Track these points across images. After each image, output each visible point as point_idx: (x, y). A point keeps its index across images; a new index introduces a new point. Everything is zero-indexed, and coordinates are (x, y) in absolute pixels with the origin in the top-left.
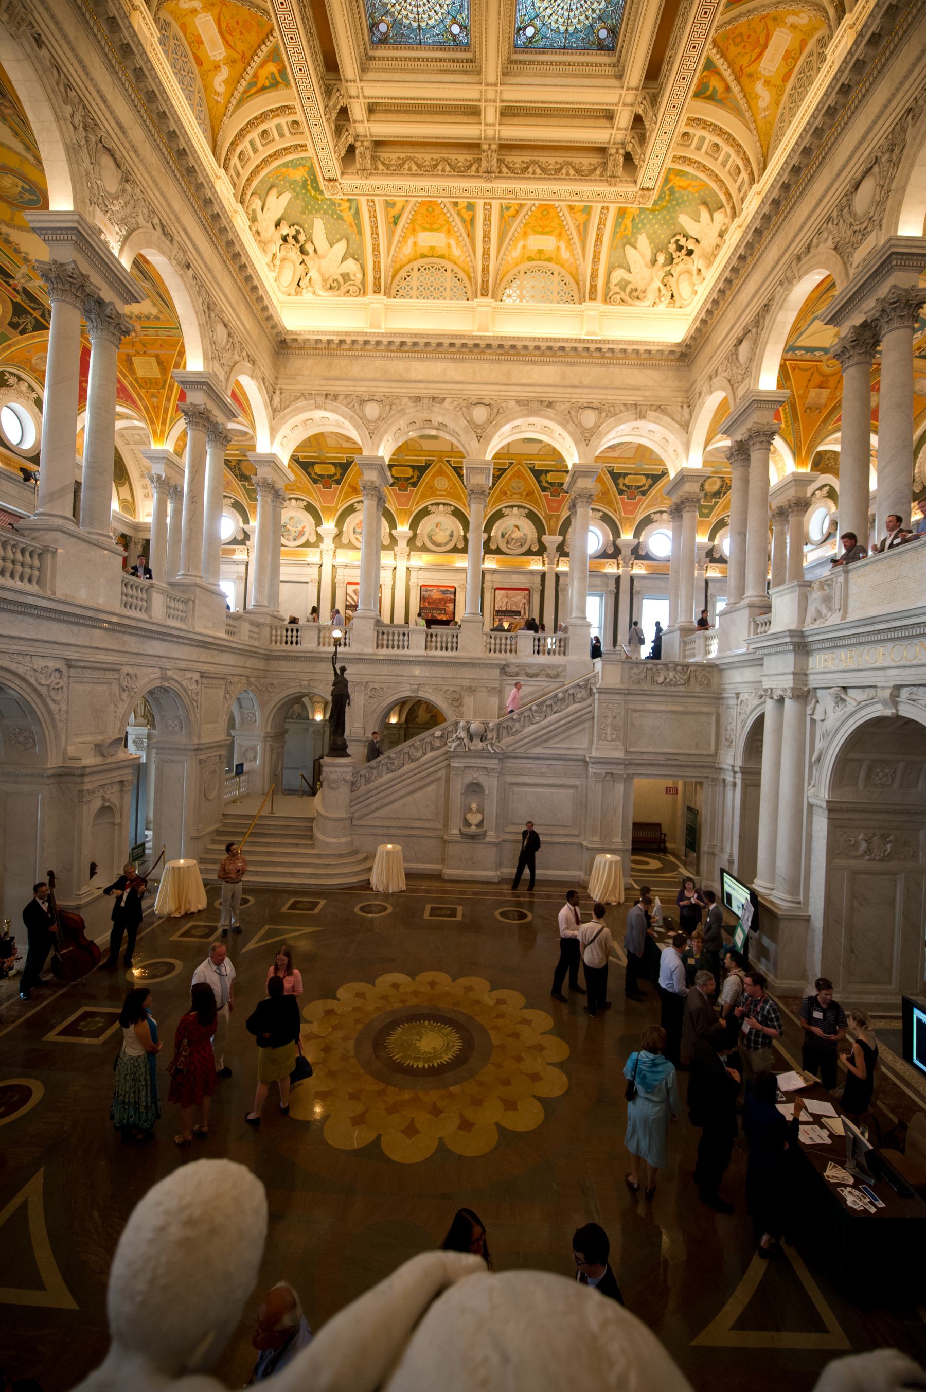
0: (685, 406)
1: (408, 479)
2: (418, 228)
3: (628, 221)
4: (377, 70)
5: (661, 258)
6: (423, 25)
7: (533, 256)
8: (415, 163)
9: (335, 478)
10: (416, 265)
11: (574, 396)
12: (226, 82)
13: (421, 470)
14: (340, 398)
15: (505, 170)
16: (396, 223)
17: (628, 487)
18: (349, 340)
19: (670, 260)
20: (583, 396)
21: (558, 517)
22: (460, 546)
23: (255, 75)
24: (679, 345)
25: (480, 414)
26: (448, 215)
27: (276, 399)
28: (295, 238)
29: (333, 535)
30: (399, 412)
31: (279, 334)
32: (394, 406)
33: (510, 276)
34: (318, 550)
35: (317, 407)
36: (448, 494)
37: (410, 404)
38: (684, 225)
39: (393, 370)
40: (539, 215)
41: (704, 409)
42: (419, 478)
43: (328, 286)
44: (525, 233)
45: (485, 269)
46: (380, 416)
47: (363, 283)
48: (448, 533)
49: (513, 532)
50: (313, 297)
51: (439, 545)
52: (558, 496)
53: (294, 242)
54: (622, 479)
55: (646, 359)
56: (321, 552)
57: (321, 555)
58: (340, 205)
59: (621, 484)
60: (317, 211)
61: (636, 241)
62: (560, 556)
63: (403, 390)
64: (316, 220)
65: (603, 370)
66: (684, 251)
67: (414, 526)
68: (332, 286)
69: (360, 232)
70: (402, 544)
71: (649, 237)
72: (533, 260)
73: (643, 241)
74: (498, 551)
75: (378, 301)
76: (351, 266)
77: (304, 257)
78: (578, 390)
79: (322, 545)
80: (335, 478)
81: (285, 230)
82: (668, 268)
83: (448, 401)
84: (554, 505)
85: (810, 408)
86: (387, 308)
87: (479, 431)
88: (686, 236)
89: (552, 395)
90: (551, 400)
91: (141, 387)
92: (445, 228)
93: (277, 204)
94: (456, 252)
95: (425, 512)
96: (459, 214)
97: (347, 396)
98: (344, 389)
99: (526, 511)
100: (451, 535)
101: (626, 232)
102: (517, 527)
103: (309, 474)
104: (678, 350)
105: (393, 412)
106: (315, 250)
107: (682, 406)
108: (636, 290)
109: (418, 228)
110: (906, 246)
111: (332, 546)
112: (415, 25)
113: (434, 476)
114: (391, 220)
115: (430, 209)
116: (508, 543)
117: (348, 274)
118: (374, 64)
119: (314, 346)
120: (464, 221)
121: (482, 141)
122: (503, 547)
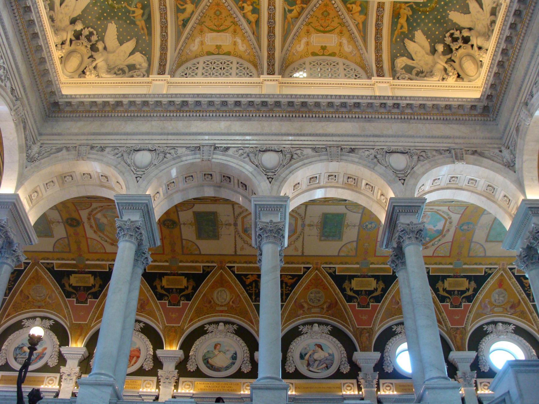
0: (503, 149)
1: (182, 290)
2: (206, 29)
3: (403, 21)
5: (440, 48)
7: (317, 51)
9: (93, 290)
11: (377, 144)
13: (197, 279)
14: (107, 150)
17: (449, 292)
18: (125, 101)
19: (448, 50)
21: (371, 332)
22: (247, 369)
24: (479, 100)
25: (270, 159)
26: (234, 16)
27: (35, 149)
29: (80, 356)
30: (174, 159)
31: (53, 93)
32: (168, 155)
33: (295, 65)
34: (58, 375)
36: (231, 310)
38: (455, 21)
39: (170, 128)
40: (320, 16)
41: (528, 138)
42: (195, 289)
44: (308, 32)
45: (271, 57)
46: (151, 164)
48: (229, 355)
49: (314, 352)
50: (97, 78)
51: (218, 370)
52: (368, 306)
54: (440, 283)
55: (449, 114)
56: (61, 377)
57: (60, 381)
59: (441, 289)
60: (112, 18)
61: (413, 36)
62: (380, 378)
64: (110, 25)
65: (405, 125)
66: (460, 41)
67: (186, 346)
70: (169, 368)
71: (425, 33)
72: (317, 55)
73: (419, 35)
74: (297, 375)
76: (139, 59)
78: (382, 139)
79: (63, 369)
80: (93, 290)
82: (449, 56)
84: (364, 318)
88: (460, 29)
90: (353, 147)
95: (200, 332)
96: (244, 16)
97: (115, 148)
99: (329, 328)
100: (234, 357)
101: (403, 30)
102: (320, 346)
103: (62, 286)
104: (480, 105)
106: (105, 48)
107: (501, 151)
108: (422, 72)
111: (77, 369)
113: (213, 288)
114: (181, 23)
115: (218, 13)
116: (308, 365)
119: (88, 108)
120: (249, 22)
122: (303, 370)
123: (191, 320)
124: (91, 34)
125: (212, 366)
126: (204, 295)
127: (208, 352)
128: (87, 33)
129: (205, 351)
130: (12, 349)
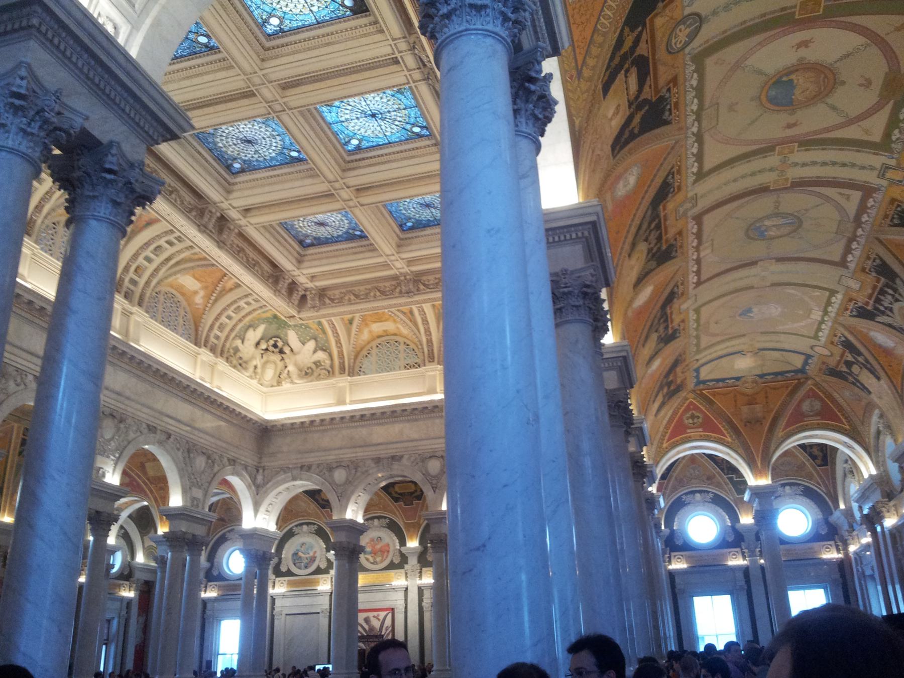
1: (412, 493)
4: (309, 261)
8: (355, 295)
10: (374, 344)
12: (203, 297)
14: (314, 467)
15: (422, 287)
27: (260, 478)
28: (275, 346)
30: (363, 473)
37: (373, 465)
45: (430, 342)
46: (347, 479)
47: (332, 366)
50: (292, 385)
63: (366, 454)
68: (307, 373)
69: (324, 332)
70: (413, 561)
75: (343, 381)
76: (321, 355)
81: (263, 346)
83: (406, 457)
85: (750, 422)
86: (351, 384)
87: (434, 482)
91: (151, 483)
93: (253, 336)
94: (405, 331)
97: (319, 465)
103: (317, 501)
105: (358, 474)
106: (292, 350)
117: (319, 362)
118: (306, 258)
120: (404, 313)
124: (276, 341)
130: (290, 556)
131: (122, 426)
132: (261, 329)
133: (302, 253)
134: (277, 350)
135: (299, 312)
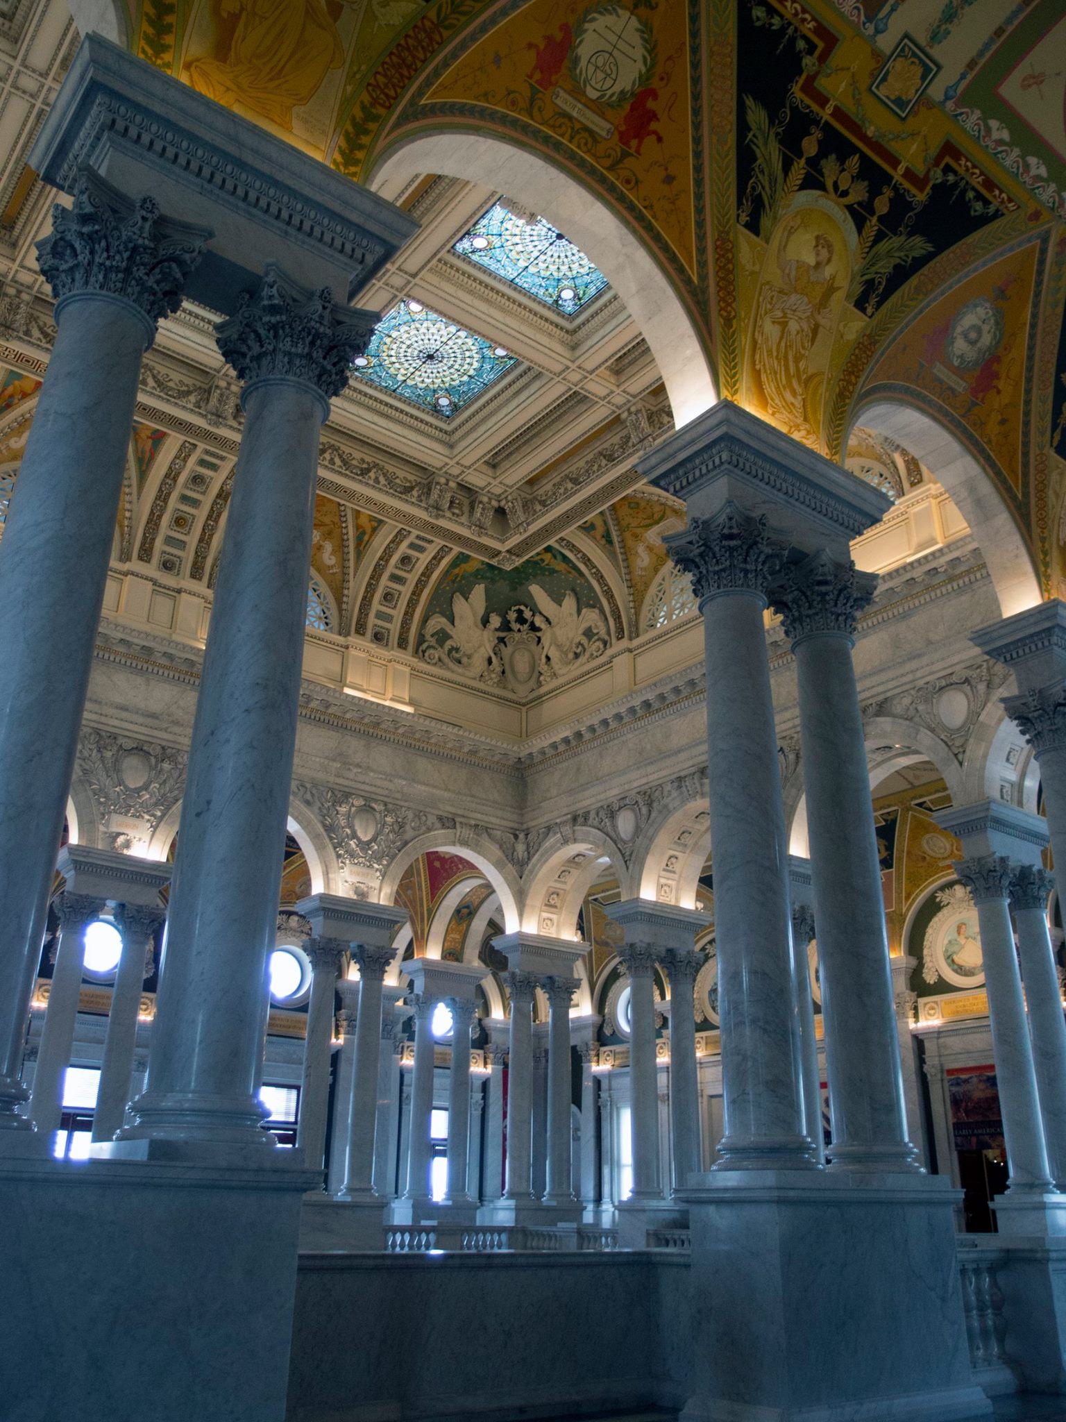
2: (639, 531)
6: (472, 372)
11: (919, 674)
12: (333, 552)
16: (610, 542)
20: (935, 668)
23: (358, 527)
28: (521, 620)
32: (655, 805)
35: (566, 842)
39: (648, 747)
43: (571, 656)
47: (609, 634)
53: (518, 626)
58: (543, 560)
76: (591, 617)
77: (538, 634)
81: (496, 621)
89: (880, 689)
90: (881, 698)
92: (668, 512)
98: (593, 800)
105: (653, 815)
106: (548, 621)
109: (639, 531)
110: (664, 460)
112: (465, 378)
113: (914, 837)
114: (603, 542)
117: (589, 629)
121: (618, 412)
123: (908, 897)
124: (520, 612)
125: (960, 967)
126: (909, 852)
127: (950, 942)
128: (515, 615)
129: (946, 942)
130: (706, 995)
131: (166, 766)
132: (479, 592)
133: (449, 428)
134: (526, 626)
135: (503, 542)
